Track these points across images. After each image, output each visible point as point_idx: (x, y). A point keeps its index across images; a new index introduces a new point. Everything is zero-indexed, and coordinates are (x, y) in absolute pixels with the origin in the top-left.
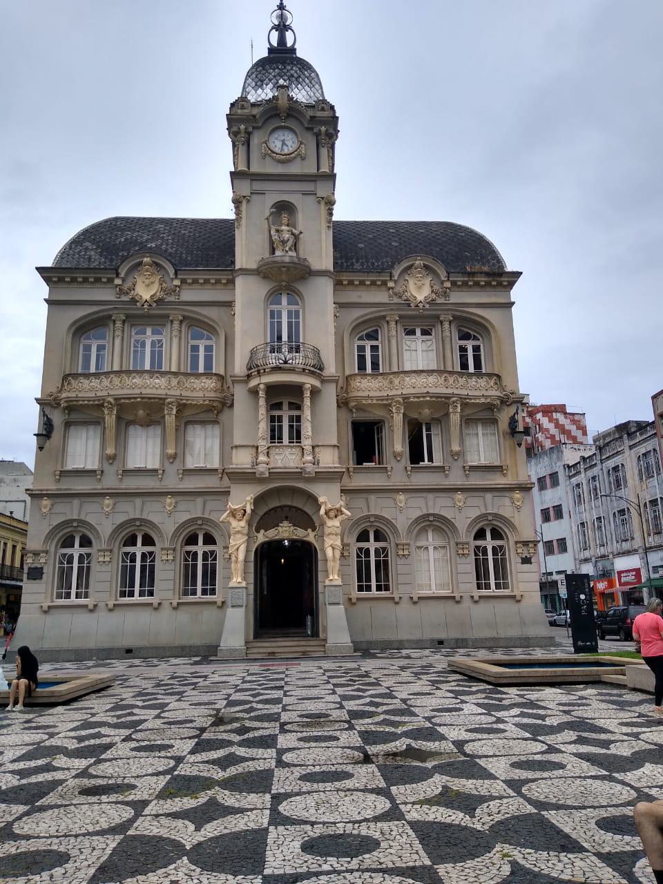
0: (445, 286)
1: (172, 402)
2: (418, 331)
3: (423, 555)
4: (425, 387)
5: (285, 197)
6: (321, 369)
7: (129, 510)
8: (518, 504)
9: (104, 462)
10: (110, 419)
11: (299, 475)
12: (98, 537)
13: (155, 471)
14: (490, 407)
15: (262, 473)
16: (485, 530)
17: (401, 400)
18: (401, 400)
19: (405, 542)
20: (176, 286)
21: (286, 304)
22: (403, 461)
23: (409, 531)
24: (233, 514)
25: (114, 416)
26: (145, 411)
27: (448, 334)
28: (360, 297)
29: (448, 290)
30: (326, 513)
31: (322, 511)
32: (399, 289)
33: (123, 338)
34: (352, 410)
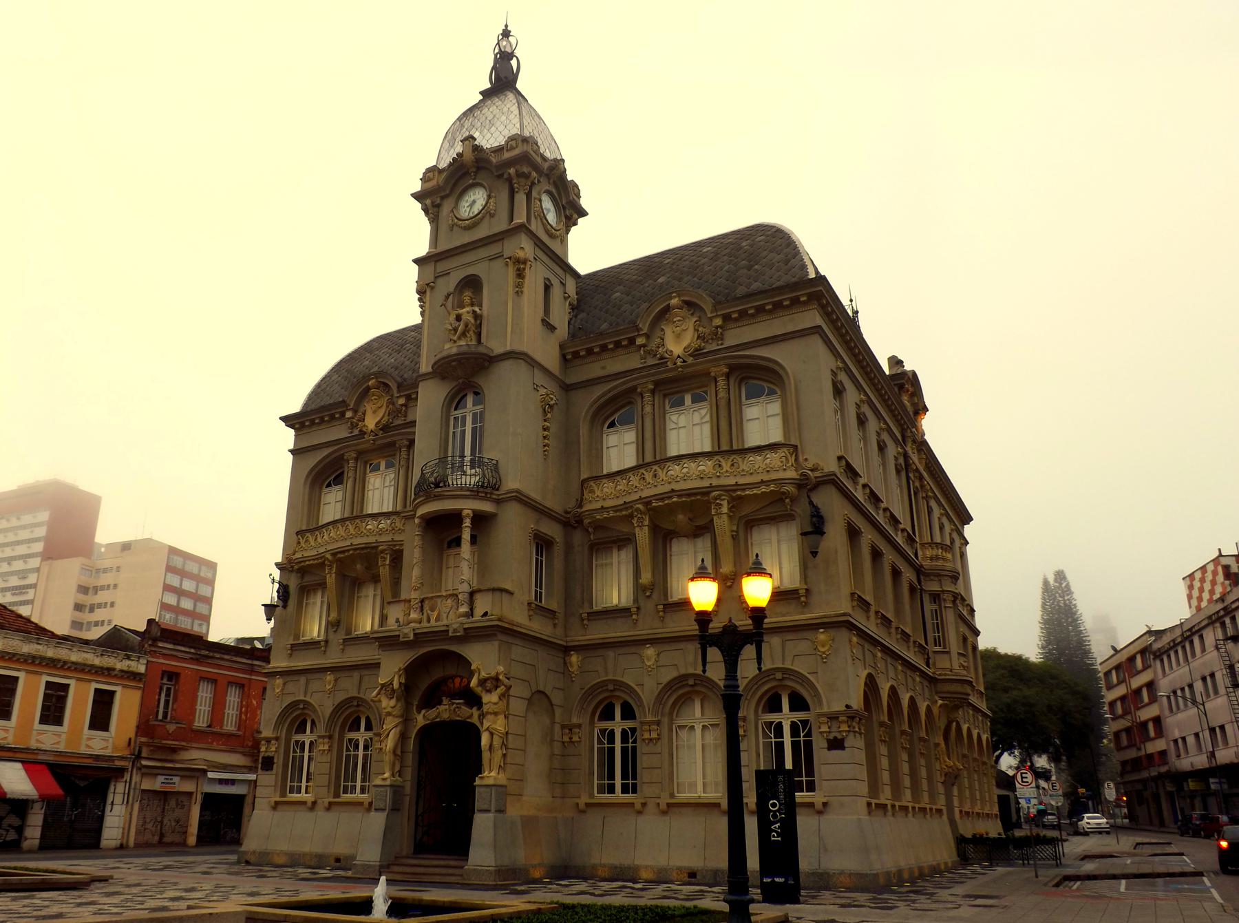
0: (714, 324)
1: (385, 550)
2: (688, 399)
3: (684, 734)
4: (670, 483)
5: (471, 271)
6: (496, 487)
8: (822, 650)
9: (331, 631)
11: (442, 635)
12: (641, 705)
14: (778, 498)
15: (406, 635)
16: (780, 696)
17: (640, 506)
18: (640, 506)
19: (649, 718)
20: (402, 405)
21: (471, 406)
22: (655, 596)
23: (660, 699)
25: (334, 575)
26: (362, 565)
27: (722, 394)
28: (603, 368)
29: (720, 330)
31: (474, 683)
32: (652, 346)
33: (355, 479)
34: (588, 530)
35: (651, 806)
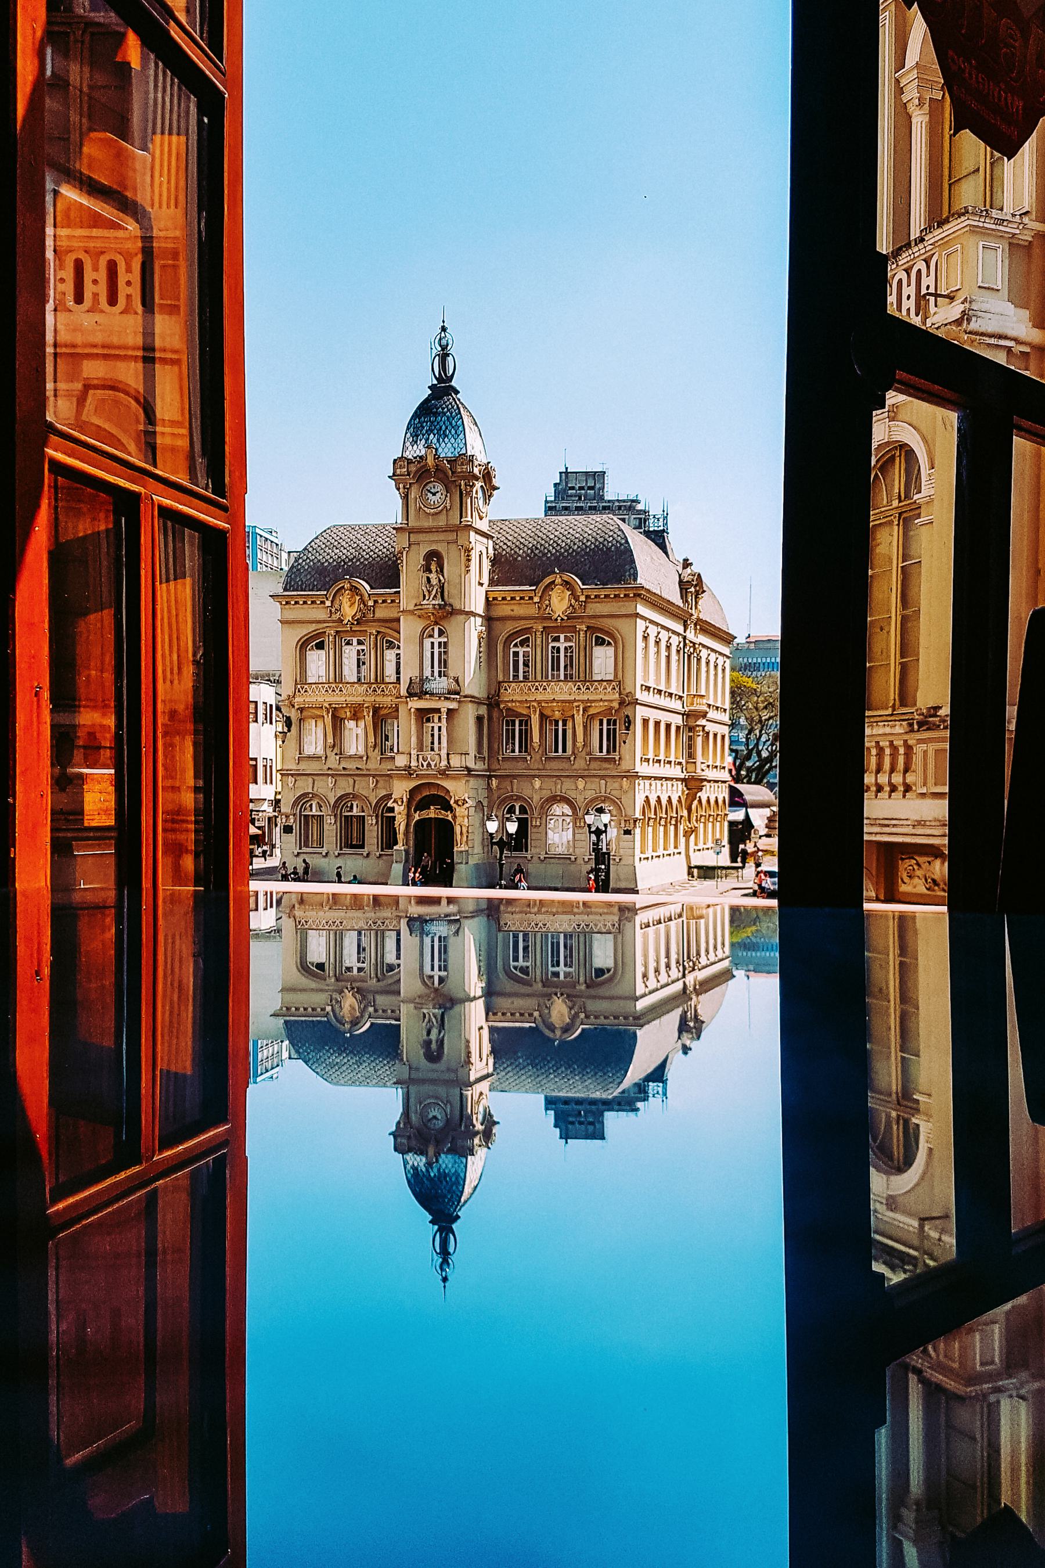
7: (345, 786)
10: (328, 719)
13: (361, 757)
24: (395, 801)
28: (513, 610)
30: (456, 802)
35: (535, 859)
